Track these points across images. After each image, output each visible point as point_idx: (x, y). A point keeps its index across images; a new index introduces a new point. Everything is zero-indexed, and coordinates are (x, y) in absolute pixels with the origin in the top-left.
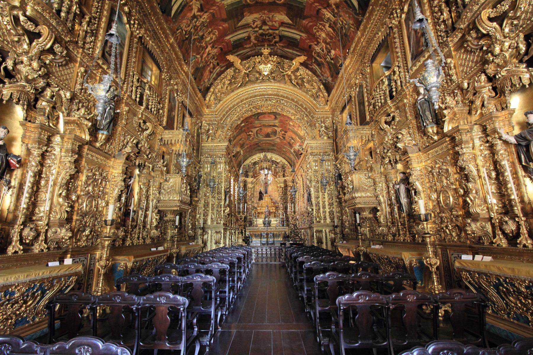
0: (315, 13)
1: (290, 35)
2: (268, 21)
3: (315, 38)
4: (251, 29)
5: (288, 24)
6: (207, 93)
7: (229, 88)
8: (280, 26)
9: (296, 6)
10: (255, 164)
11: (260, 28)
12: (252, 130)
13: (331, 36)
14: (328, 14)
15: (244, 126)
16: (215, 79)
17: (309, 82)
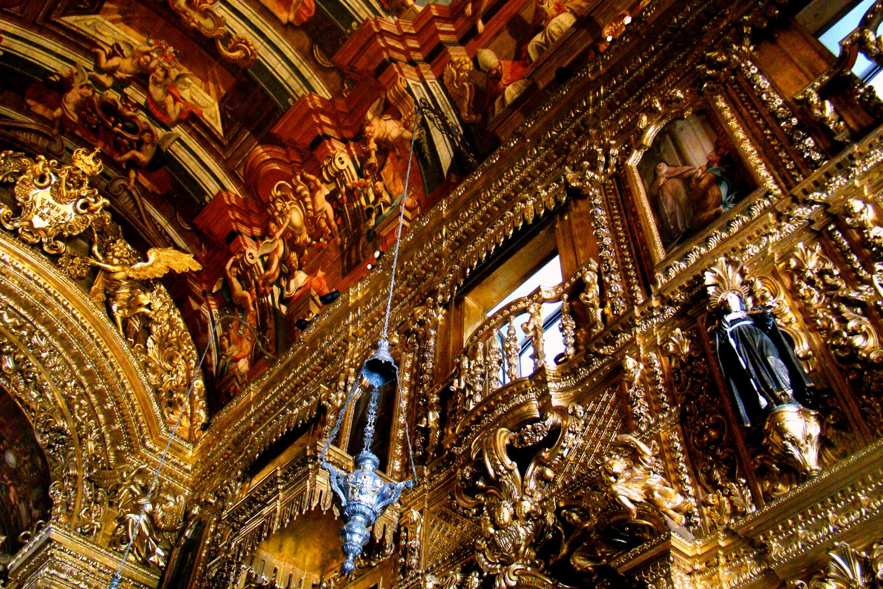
0: (308, 141)
1: (192, 165)
2: (156, 83)
3: (262, 215)
4: (90, 65)
5: (208, 130)
8: (179, 121)
9: (262, 90)
11: (120, 85)
13: (318, 227)
14: (342, 159)
17: (163, 343)
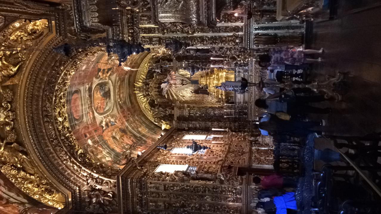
6: (42, 203)
7: (32, 172)
10: (152, 104)
12: (98, 123)
15: (92, 138)
16: (19, 192)
